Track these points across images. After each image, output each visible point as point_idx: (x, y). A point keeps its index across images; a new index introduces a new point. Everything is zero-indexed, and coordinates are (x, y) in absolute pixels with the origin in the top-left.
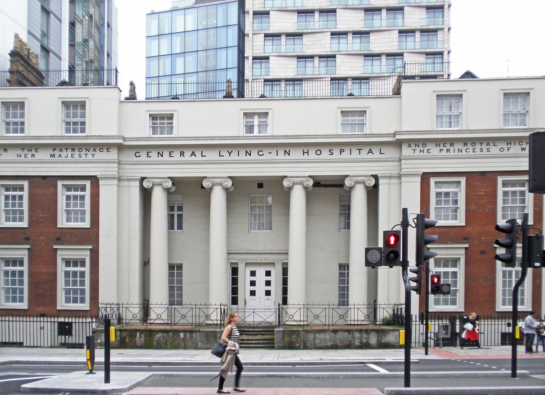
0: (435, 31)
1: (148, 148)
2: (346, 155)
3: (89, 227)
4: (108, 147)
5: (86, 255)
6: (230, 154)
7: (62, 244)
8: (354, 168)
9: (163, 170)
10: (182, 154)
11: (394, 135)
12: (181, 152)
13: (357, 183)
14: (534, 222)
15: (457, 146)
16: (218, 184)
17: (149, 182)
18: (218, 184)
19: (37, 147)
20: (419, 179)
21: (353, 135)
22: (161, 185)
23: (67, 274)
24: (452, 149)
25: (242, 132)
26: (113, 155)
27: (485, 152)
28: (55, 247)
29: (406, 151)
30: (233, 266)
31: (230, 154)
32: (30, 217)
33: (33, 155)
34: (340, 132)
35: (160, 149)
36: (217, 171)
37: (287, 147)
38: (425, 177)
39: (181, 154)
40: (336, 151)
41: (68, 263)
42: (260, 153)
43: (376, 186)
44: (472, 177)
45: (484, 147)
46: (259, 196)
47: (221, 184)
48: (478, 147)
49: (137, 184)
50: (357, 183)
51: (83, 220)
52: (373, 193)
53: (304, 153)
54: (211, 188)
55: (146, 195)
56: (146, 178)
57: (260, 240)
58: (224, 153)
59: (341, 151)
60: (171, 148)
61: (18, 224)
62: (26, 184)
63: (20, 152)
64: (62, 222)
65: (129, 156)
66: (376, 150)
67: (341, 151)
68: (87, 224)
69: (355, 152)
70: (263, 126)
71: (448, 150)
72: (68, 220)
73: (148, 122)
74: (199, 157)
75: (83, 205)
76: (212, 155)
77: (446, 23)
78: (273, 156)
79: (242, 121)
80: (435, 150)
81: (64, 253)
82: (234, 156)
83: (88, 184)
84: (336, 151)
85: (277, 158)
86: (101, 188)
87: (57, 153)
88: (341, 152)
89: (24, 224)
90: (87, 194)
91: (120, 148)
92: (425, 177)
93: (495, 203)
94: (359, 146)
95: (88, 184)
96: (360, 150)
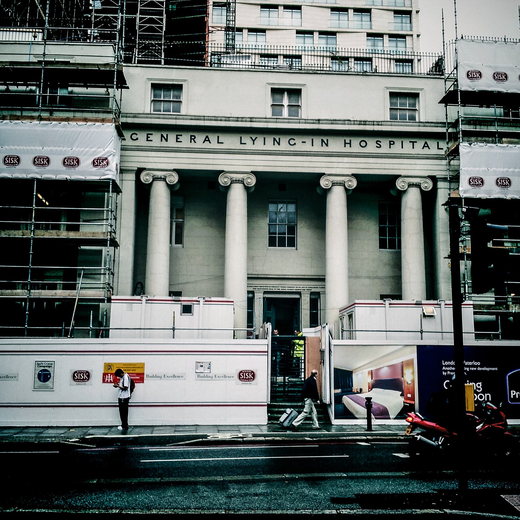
0: (404, 36)
2: (397, 149)
6: (254, 141)
12: (191, 136)
13: (410, 185)
17: (148, 175)
22: (164, 180)
30: (313, 297)
31: (254, 141)
36: (238, 164)
39: (191, 139)
42: (292, 142)
43: (435, 189)
47: (242, 182)
49: (132, 177)
50: (410, 185)
53: (345, 143)
55: (143, 193)
56: (144, 169)
59: (391, 144)
67: (391, 144)
70: (295, 108)
73: (149, 94)
74: (214, 145)
76: (230, 142)
77: (414, 29)
78: (307, 147)
82: (259, 145)
88: (390, 144)
96: (413, 142)
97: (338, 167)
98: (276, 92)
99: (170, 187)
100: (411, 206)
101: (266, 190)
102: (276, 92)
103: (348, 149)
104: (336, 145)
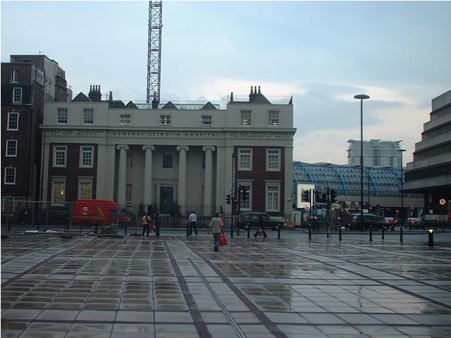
4: (103, 130)
8: (207, 143)
9: (125, 141)
10: (134, 134)
15: (249, 134)
20: (233, 149)
21: (207, 127)
26: (104, 134)
29: (228, 136)
36: (149, 142)
37: (178, 132)
38: (236, 148)
41: (82, 183)
44: (254, 148)
45: (260, 135)
49: (114, 147)
52: (214, 154)
55: (118, 152)
57: (166, 174)
59: (201, 134)
62: (66, 147)
63: (77, 132)
64: (82, 166)
65: (111, 134)
66: (216, 134)
69: (207, 135)
76: (147, 135)
78: (172, 136)
80: (240, 136)
83: (93, 147)
91: (107, 130)
92: (236, 148)
94: (209, 132)
95: (93, 147)
97: (183, 143)
98: (163, 117)
100: (209, 156)
101: (158, 150)
102: (163, 117)
103: (186, 136)
104: (182, 136)
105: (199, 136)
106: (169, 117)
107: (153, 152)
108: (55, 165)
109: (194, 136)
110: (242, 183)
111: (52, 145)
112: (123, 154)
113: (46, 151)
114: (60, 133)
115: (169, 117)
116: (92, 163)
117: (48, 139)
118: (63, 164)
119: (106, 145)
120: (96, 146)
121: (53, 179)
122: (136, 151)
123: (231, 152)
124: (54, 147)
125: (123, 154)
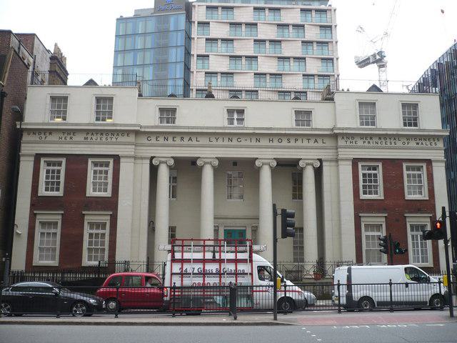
1: (157, 134)
2: (299, 143)
3: (110, 196)
4: (128, 132)
5: (106, 219)
7: (89, 210)
8: (306, 154)
9: (167, 152)
10: (182, 139)
11: (332, 130)
13: (307, 164)
14: (430, 198)
16: (208, 163)
18: (208, 163)
19: (74, 132)
23: (91, 235)
24: (371, 141)
25: (226, 124)
26: (132, 138)
27: (393, 145)
28: (83, 213)
29: (341, 142)
32: (65, 187)
33: (71, 138)
34: (294, 126)
35: (166, 135)
36: (207, 153)
38: (355, 162)
40: (292, 141)
41: (92, 225)
42: (239, 140)
43: (321, 167)
44: (384, 161)
45: (393, 141)
46: (237, 173)
47: (210, 163)
48: (388, 140)
49: (148, 161)
50: (307, 164)
51: (105, 190)
52: (318, 173)
54: (202, 167)
55: (154, 171)
57: (237, 209)
58: (213, 139)
59: (296, 140)
60: (174, 134)
61: (55, 193)
62: (64, 161)
64: (90, 192)
65: (143, 140)
66: (320, 141)
68: (108, 194)
70: (241, 120)
71: (369, 142)
72: (94, 190)
74: (194, 142)
75: (106, 178)
76: (204, 141)
78: (248, 143)
79: (226, 116)
80: (360, 143)
81: (90, 217)
82: (220, 142)
84: (292, 141)
85: (251, 144)
86: (122, 165)
87: (89, 136)
89: (60, 193)
90: (110, 169)
91: (137, 133)
92: (355, 162)
93: (403, 183)
94: (308, 137)
95: (111, 161)
97: (266, 155)
98: (230, 112)
99: (170, 168)
102: (230, 112)
103: (271, 144)
104: (264, 142)
105: (292, 143)
106: (241, 112)
107: (216, 171)
108: (42, 192)
109: (285, 143)
110: (367, 219)
111: (38, 157)
112: (164, 174)
113: (26, 168)
114: (54, 137)
115: (241, 112)
116: (110, 187)
117: (29, 148)
118: (58, 190)
119: (135, 158)
120: (117, 158)
121: (38, 217)
122: (186, 169)
123: (346, 170)
124: (42, 160)
125: (164, 174)
